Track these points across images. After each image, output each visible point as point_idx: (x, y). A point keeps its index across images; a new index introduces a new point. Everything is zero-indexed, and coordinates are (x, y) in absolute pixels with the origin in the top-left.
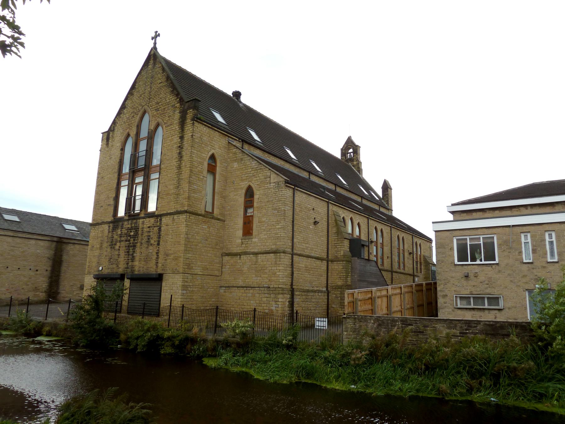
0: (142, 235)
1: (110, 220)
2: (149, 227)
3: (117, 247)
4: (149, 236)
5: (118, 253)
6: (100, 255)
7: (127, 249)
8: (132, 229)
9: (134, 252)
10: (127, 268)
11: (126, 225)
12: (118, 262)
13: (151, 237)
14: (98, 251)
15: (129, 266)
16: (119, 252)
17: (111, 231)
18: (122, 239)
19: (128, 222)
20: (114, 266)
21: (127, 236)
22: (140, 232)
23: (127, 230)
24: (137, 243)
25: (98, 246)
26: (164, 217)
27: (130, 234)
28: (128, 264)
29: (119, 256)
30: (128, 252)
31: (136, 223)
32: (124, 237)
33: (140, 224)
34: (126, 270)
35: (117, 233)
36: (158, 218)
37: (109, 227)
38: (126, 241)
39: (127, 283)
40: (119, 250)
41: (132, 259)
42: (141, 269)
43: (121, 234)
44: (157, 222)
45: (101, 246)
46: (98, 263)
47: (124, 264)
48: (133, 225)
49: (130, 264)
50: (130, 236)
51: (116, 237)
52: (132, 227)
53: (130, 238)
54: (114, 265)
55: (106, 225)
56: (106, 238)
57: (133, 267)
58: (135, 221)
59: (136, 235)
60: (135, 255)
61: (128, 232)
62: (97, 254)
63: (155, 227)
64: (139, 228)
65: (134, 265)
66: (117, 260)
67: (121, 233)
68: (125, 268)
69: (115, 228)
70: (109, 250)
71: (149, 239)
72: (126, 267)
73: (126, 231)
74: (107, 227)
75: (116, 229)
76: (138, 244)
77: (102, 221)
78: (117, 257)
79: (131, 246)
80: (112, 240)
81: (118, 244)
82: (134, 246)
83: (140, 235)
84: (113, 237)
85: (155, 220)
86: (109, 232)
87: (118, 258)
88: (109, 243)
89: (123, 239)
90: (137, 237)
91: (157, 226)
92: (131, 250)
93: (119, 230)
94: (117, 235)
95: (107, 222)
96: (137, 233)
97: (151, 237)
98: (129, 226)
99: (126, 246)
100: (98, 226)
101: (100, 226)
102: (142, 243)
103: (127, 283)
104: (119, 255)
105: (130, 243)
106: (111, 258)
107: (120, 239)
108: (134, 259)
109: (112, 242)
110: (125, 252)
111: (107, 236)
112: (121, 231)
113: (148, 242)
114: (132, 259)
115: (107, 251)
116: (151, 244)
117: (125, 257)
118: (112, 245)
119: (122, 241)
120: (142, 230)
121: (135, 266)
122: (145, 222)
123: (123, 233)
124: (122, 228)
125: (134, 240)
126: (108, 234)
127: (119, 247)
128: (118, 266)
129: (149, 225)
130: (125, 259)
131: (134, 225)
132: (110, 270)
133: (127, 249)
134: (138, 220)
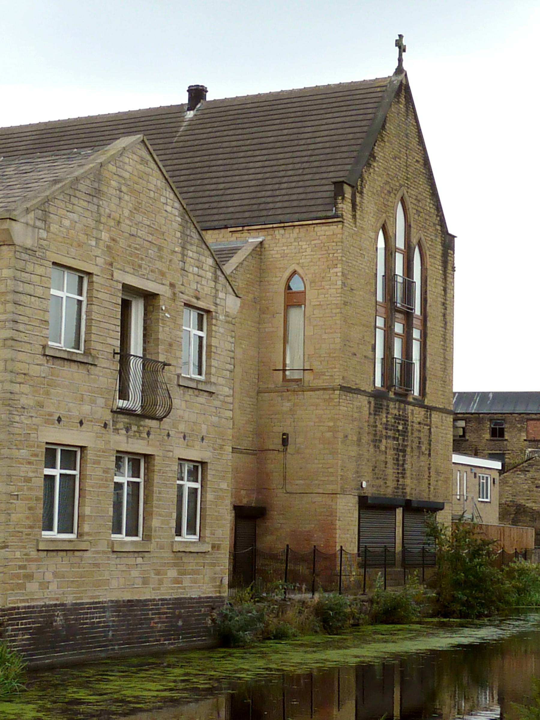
0: (412, 434)
1: (370, 391)
2: (419, 423)
3: (383, 448)
4: (420, 438)
5: (383, 459)
6: (360, 457)
7: (396, 454)
8: (400, 419)
9: (404, 460)
10: (397, 488)
11: (392, 409)
12: (385, 475)
13: (422, 440)
14: (355, 448)
15: (401, 485)
16: (386, 457)
17: (372, 412)
18: (389, 434)
19: (395, 404)
20: (381, 482)
21: (394, 430)
22: (409, 428)
23: (394, 418)
24: (406, 446)
25: (355, 438)
26: (435, 412)
27: (397, 427)
28: (398, 481)
29: (386, 464)
30: (397, 460)
31: (404, 410)
32: (391, 430)
33: (409, 414)
34: (397, 492)
35: (381, 419)
36: (427, 411)
37: (369, 403)
38: (395, 439)
39: (399, 512)
40: (386, 453)
41: (402, 473)
42: (414, 492)
43: (386, 424)
44: (427, 418)
45: (359, 440)
46: (357, 472)
47: (393, 480)
48: (401, 413)
49: (401, 480)
50: (398, 431)
51: (380, 427)
52: (399, 415)
53: (399, 435)
54: (381, 480)
55: (364, 397)
56: (366, 424)
57: (404, 487)
58: (402, 405)
59: (404, 433)
60: (406, 466)
61: (395, 422)
62: (353, 454)
63: (425, 425)
64: (408, 421)
65: (405, 483)
66: (384, 471)
67: (387, 421)
68: (395, 488)
69: (377, 410)
70: (372, 450)
71: (419, 443)
72: (396, 486)
73: (393, 421)
74: (366, 402)
75: (379, 412)
76: (408, 449)
77: (357, 386)
78: (384, 466)
79: (401, 451)
80: (375, 431)
81: (384, 441)
82: (404, 451)
83: (410, 434)
84: (376, 426)
85: (425, 414)
86: (370, 414)
87: (386, 467)
88: (371, 437)
89: (390, 433)
90: (407, 436)
91: (427, 425)
92: (401, 458)
93: (384, 415)
94: (381, 424)
95: (364, 391)
96: (407, 428)
97: (422, 440)
98: (396, 412)
99: (394, 449)
100: (351, 395)
101: (355, 396)
102: (412, 448)
103: (399, 512)
104: (386, 463)
105: (399, 444)
106: (376, 467)
107: (387, 432)
108: (405, 473)
109: (375, 435)
110: (393, 459)
111: (368, 421)
112: (387, 417)
113: (419, 447)
114: (402, 473)
115: (368, 451)
116: (423, 452)
117: (394, 469)
118: (376, 442)
119: (389, 437)
120: (412, 426)
121: (407, 485)
122: (415, 412)
123: (389, 423)
124: (388, 413)
125: (404, 440)
126: (369, 418)
127: (386, 448)
128: (386, 483)
129: (419, 420)
130: (394, 472)
131: (403, 413)
132: (375, 489)
133: (396, 454)
134: (407, 406)
